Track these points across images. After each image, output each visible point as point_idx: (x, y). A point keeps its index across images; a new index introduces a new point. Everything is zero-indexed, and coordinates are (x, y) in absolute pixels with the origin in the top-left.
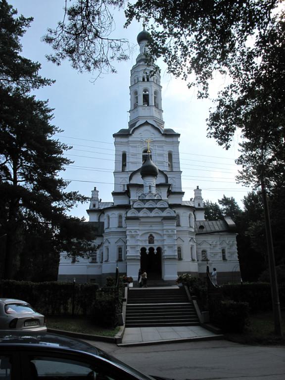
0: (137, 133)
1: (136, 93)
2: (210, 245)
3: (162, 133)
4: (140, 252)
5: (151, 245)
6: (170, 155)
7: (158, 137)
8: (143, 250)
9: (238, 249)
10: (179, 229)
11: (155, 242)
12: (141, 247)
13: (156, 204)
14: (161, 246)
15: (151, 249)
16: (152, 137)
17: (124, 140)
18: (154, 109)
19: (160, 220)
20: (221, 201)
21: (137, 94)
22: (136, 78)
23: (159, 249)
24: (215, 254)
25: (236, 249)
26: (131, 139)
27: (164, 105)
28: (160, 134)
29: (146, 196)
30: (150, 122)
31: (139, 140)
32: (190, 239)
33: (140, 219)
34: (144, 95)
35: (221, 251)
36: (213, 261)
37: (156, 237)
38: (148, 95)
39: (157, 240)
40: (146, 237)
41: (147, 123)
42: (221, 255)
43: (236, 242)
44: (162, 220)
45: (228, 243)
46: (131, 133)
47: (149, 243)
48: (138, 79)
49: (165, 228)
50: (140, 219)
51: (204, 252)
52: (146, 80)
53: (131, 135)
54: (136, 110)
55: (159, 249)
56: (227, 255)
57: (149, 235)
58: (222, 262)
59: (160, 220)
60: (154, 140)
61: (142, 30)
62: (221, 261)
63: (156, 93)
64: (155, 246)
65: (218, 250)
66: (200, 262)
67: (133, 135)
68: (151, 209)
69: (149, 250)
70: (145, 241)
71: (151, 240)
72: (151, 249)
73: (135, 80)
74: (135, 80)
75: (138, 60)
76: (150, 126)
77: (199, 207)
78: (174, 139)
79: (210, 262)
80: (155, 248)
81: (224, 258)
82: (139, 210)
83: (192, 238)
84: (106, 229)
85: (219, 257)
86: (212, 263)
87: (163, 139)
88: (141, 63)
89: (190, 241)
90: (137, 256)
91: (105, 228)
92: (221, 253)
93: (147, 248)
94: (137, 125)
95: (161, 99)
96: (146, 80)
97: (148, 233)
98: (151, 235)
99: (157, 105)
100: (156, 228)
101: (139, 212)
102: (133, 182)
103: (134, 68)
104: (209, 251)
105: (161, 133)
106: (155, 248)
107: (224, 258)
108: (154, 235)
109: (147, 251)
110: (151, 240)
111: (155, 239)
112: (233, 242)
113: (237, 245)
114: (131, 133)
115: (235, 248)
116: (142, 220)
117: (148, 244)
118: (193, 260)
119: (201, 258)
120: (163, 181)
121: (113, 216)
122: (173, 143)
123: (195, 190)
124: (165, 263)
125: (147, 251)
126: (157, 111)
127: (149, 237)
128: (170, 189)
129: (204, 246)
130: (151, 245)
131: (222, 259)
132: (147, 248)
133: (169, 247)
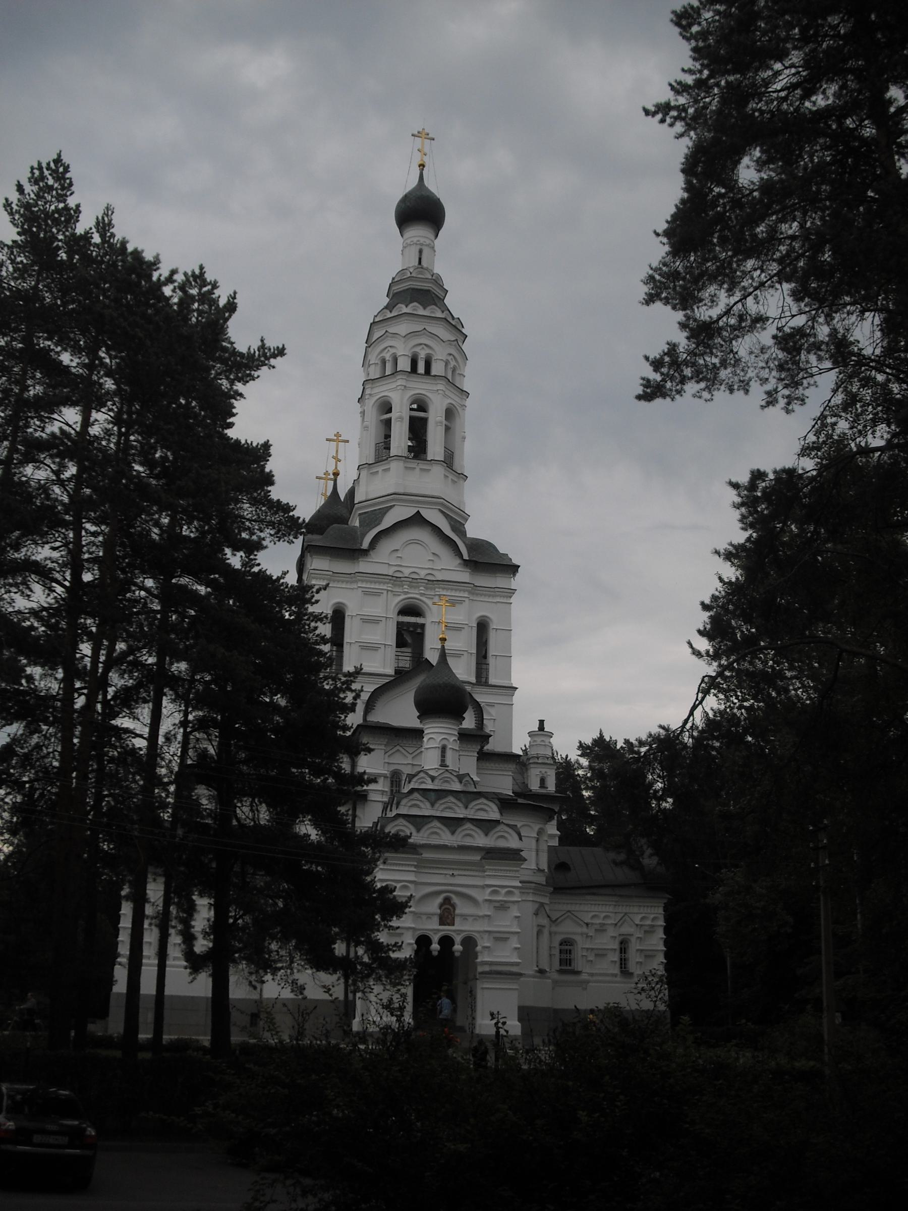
0: (386, 547)
1: (386, 407)
2: (587, 924)
3: (466, 557)
5: (447, 929)
6: (482, 627)
7: (448, 566)
8: (423, 941)
9: (666, 943)
11: (457, 920)
12: (418, 933)
13: (466, 808)
14: (477, 936)
15: (447, 941)
18: (438, 471)
19: (479, 858)
20: (588, 747)
21: (390, 410)
22: (388, 356)
23: (469, 942)
24: (601, 954)
25: (662, 943)
26: (363, 566)
27: (469, 455)
28: (459, 561)
30: (432, 516)
32: (537, 906)
33: (420, 850)
34: (412, 419)
35: (616, 946)
36: (592, 975)
37: (462, 908)
38: (424, 421)
39: (465, 917)
40: (434, 906)
41: (418, 520)
42: (616, 957)
43: (661, 922)
44: (483, 858)
45: (637, 922)
47: (442, 922)
50: (420, 850)
51: (567, 946)
52: (421, 369)
53: (365, 553)
54: (380, 468)
56: (634, 957)
57: (440, 899)
58: (618, 979)
62: (615, 975)
63: (450, 413)
64: (459, 932)
65: (608, 942)
66: (556, 976)
67: (371, 552)
68: (453, 823)
69: (439, 943)
70: (429, 916)
71: (447, 915)
72: (447, 941)
73: (384, 362)
74: (384, 362)
75: (396, 288)
76: (429, 529)
77: (543, 791)
78: (500, 581)
79: (584, 977)
81: (625, 972)
83: (542, 905)
85: (609, 965)
86: (588, 982)
87: (464, 576)
89: (536, 914)
92: (618, 952)
93: (435, 938)
94: (388, 521)
95: (464, 438)
96: (421, 369)
97: (438, 893)
98: (447, 900)
99: (449, 461)
100: (464, 880)
102: (374, 718)
104: (582, 944)
105: (459, 554)
106: (458, 939)
107: (625, 972)
108: (455, 900)
110: (447, 915)
111: (457, 912)
112: (654, 919)
113: (667, 930)
114: (365, 545)
115: (657, 942)
116: (427, 855)
118: (541, 972)
119: (556, 965)
122: (493, 592)
123: (531, 734)
125: (435, 947)
126: (451, 477)
127: (441, 906)
129: (568, 928)
130: (447, 929)
131: (617, 971)
132: (435, 938)
133: (496, 939)
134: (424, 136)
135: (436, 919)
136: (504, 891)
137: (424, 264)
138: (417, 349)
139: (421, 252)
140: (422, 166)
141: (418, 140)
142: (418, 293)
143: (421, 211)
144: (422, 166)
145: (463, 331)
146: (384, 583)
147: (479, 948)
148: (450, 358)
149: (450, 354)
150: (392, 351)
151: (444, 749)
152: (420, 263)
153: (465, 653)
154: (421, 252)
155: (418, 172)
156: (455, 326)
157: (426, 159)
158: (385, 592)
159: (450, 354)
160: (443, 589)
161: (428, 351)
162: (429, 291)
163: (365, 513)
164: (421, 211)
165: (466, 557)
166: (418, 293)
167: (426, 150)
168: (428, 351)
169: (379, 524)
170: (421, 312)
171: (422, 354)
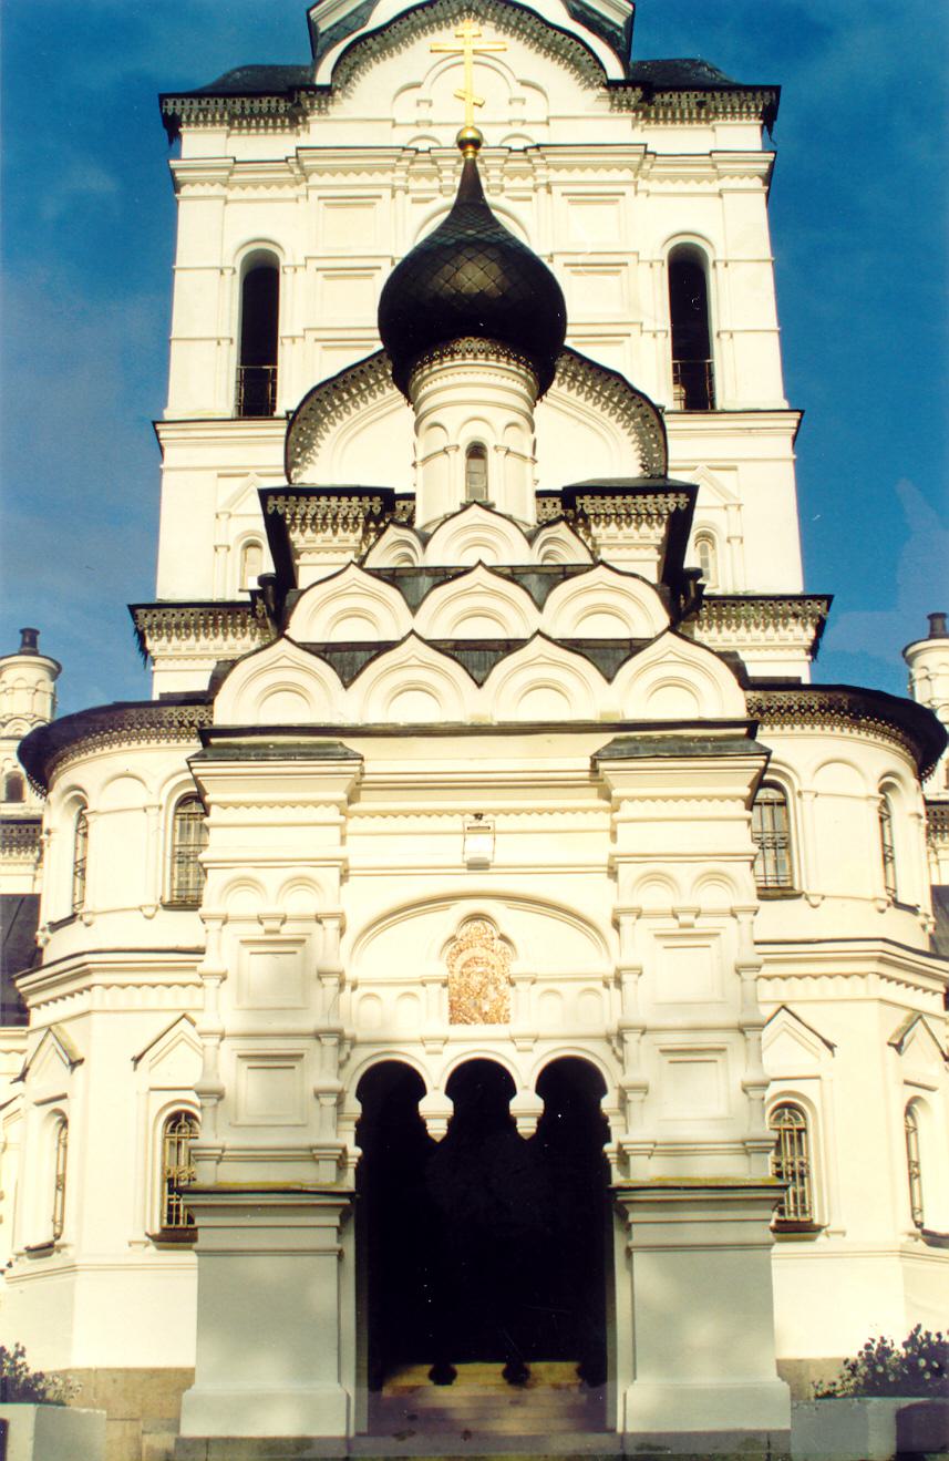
4: (354, 1108)
5: (478, 1042)
10: (780, 919)
12: (362, 1060)
14: (598, 1055)
16: (517, 112)
17: (273, 144)
23: (572, 1084)
26: (321, 129)
29: (425, 540)
31: (401, 137)
32: (900, 1018)
46: (323, 77)
47: (457, 1015)
49: (630, 839)
55: (572, 1084)
59: (575, 754)
60: (540, 135)
68: (477, 656)
80: (525, 1072)
82: (348, 659)
83: (918, 1016)
84: (55, 926)
87: (621, 127)
90: (312, 1155)
91: (43, 923)
93: (435, 1073)
101: (348, 676)
106: (525, 1072)
109: (436, 1111)
116: (380, 758)
117: (439, 1025)
120: (619, 459)
121: (129, 793)
124: (640, 1235)
128: (691, 560)
132: (435, 1073)
135: (438, 999)
136: (684, 873)
146: (383, 170)
147: (608, 1104)
151: (476, 451)
153: (634, 330)
158: (387, 193)
160: (558, 168)
163: (337, 25)
165: (615, 71)
169: (363, 26)
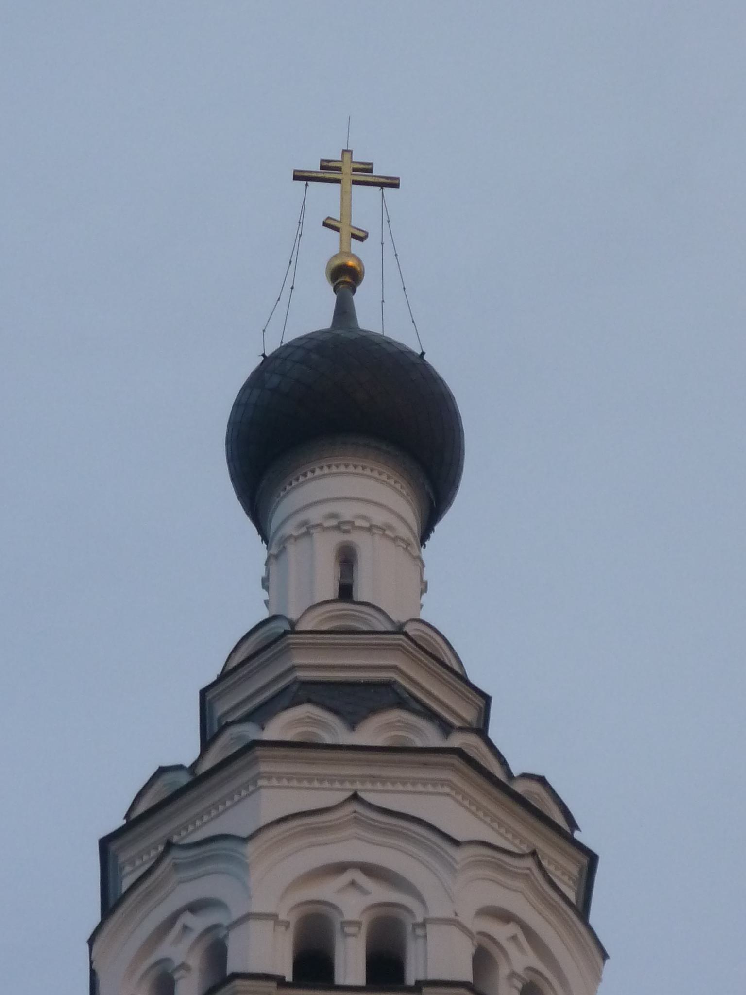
22: (183, 952)
48: (217, 953)
61: (312, 312)
88: (280, 727)
103: (168, 797)
134: (347, 175)
137: (362, 592)
138: (327, 890)
139: (347, 559)
140: (345, 277)
141: (325, 198)
142: (333, 692)
143: (343, 411)
144: (345, 277)
145: (577, 835)
148: (502, 932)
149: (506, 917)
150: (199, 923)
152: (345, 592)
154: (347, 559)
155: (333, 298)
156: (538, 812)
157: (364, 254)
159: (506, 917)
161: (380, 893)
162: (388, 685)
164: (343, 411)
166: (333, 692)
167: (358, 221)
168: (380, 893)
170: (335, 731)
171: (354, 906)
